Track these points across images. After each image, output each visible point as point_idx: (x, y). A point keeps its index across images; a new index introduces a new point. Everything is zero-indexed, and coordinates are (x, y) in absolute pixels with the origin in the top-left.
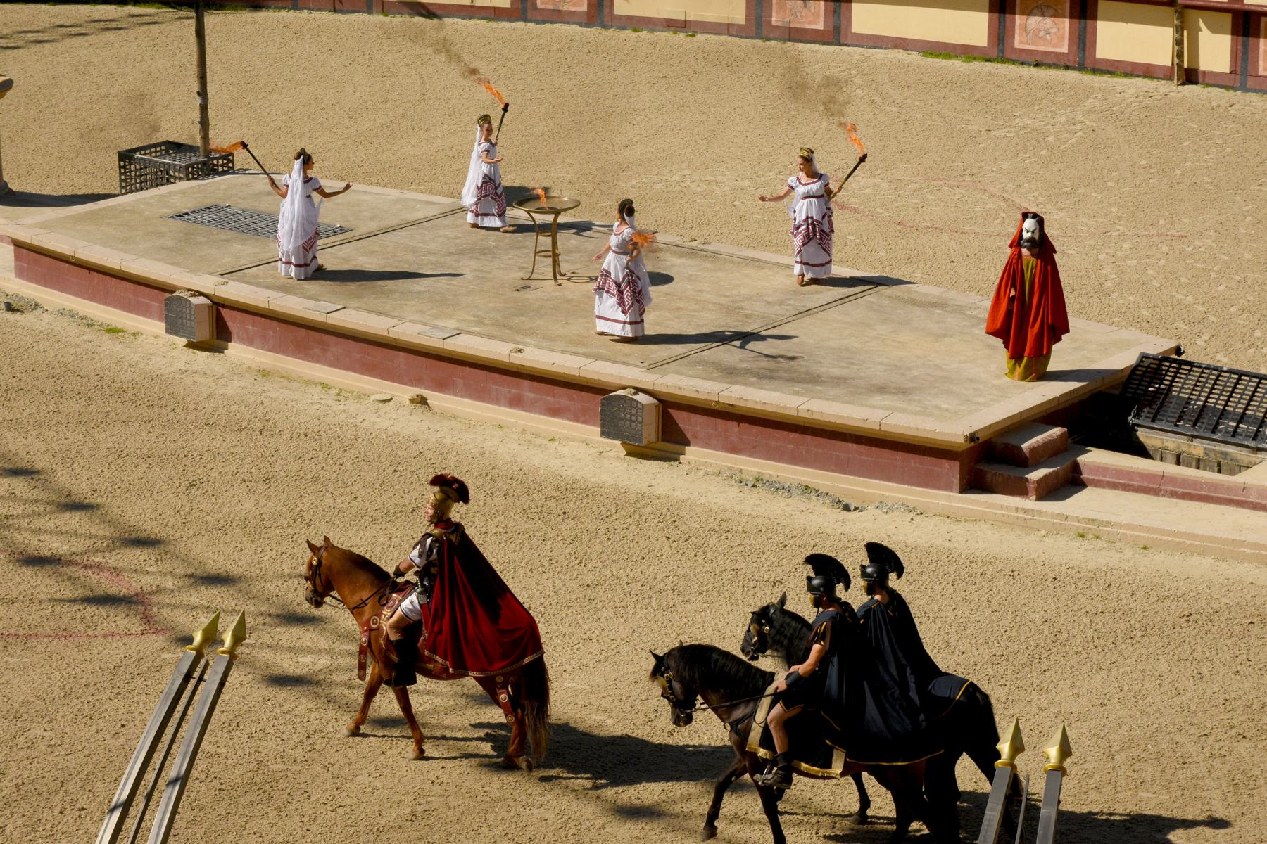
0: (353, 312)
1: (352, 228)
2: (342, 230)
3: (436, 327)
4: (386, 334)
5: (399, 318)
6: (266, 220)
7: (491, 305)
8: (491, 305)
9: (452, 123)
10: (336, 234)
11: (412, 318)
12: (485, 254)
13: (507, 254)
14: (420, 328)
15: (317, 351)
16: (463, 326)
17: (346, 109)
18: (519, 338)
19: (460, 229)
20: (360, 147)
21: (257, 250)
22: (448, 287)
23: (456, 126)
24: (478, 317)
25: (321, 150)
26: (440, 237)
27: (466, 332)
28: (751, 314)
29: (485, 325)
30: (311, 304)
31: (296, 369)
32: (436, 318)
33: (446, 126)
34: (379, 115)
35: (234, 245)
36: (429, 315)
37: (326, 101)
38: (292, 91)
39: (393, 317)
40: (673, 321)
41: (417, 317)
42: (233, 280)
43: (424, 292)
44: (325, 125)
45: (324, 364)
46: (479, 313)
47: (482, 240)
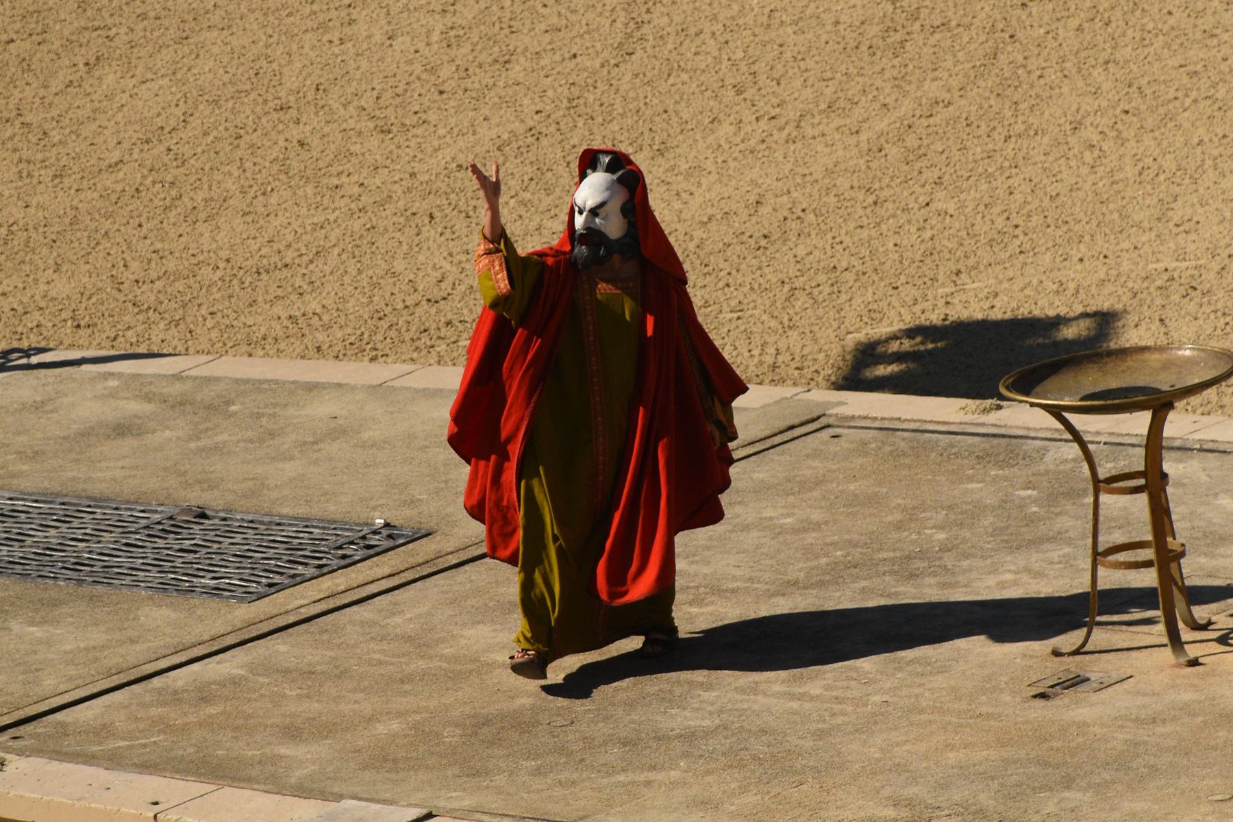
1: (426, 527)
6: (121, 524)
7: (952, 757)
8: (952, 757)
9: (748, 116)
10: (372, 552)
12: (913, 576)
13: (994, 571)
17: (367, 101)
19: (816, 494)
20: (429, 232)
21: (97, 636)
22: (795, 705)
23: (763, 124)
24: (910, 803)
25: (290, 256)
33: (726, 129)
34: (486, 111)
35: (15, 626)
37: (291, 82)
38: (167, 55)
42: (20, 753)
43: (708, 733)
44: (295, 165)
46: (912, 791)
47: (899, 526)
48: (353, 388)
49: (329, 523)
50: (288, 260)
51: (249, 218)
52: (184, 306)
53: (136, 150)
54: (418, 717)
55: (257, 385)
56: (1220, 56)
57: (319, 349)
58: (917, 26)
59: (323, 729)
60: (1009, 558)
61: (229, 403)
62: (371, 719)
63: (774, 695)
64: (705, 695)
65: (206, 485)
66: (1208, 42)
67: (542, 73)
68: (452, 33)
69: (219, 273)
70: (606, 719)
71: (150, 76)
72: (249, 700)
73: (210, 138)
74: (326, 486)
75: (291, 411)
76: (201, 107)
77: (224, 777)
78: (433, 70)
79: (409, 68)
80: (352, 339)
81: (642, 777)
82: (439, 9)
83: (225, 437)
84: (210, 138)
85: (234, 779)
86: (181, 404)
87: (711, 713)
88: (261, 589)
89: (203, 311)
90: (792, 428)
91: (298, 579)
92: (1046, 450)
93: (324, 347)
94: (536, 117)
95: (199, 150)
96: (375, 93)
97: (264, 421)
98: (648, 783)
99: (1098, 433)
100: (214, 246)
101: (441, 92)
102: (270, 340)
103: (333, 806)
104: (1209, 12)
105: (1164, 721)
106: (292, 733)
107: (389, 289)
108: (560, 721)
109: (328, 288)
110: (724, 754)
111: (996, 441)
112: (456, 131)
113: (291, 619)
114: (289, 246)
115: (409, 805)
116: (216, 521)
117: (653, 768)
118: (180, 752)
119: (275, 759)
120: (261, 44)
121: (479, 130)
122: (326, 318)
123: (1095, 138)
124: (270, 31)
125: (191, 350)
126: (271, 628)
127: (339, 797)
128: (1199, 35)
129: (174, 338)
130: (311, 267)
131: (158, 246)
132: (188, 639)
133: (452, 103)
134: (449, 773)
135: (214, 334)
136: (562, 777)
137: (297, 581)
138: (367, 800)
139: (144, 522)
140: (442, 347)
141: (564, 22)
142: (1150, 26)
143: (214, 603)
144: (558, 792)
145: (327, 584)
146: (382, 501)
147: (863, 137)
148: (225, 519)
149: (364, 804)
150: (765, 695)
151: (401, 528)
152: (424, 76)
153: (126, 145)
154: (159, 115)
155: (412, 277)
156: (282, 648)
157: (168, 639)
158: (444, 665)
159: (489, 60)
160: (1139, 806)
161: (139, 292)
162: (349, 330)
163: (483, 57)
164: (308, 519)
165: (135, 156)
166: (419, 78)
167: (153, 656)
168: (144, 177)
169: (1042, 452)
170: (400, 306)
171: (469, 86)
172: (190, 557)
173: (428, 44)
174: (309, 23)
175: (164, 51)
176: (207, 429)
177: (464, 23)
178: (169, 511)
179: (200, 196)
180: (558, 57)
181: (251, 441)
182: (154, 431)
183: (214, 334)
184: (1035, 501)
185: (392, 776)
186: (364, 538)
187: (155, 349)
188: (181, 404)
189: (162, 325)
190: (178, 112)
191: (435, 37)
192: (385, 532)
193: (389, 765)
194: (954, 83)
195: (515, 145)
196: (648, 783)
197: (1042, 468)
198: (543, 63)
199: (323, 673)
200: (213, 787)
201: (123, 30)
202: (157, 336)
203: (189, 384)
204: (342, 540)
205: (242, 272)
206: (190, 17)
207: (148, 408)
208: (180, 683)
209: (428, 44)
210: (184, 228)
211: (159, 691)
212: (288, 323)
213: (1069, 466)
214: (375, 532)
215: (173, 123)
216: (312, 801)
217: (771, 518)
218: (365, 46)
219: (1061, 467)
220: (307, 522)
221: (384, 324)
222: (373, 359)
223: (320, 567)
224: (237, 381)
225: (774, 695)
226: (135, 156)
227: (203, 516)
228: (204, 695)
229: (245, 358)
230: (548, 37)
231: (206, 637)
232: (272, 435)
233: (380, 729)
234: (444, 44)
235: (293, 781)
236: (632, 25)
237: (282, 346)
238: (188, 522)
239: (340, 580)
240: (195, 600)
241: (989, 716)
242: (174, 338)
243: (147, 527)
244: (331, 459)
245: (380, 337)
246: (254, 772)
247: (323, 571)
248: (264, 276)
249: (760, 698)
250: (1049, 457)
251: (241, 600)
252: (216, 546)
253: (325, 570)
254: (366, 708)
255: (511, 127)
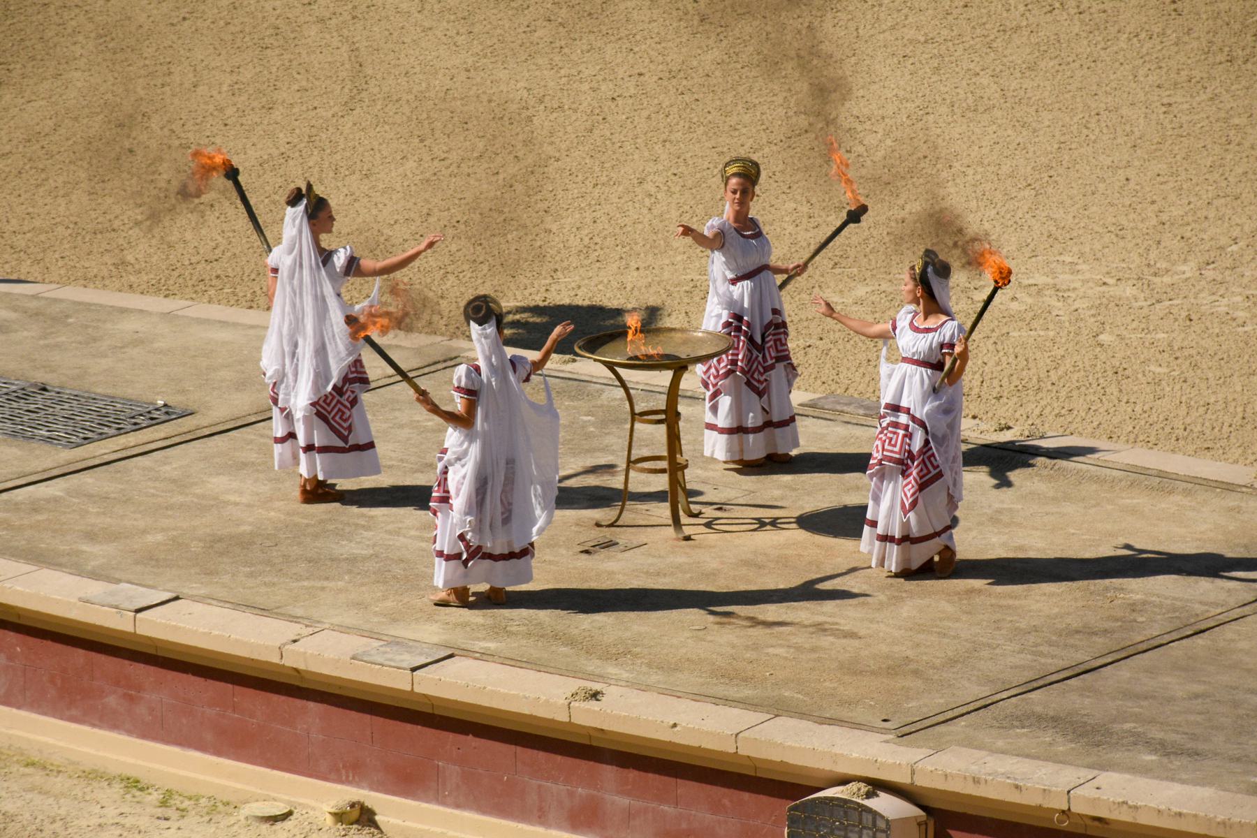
0: (198, 608)
1: (190, 409)
2: (170, 413)
3: (397, 642)
4: (275, 659)
5: (309, 621)
9: (427, 157)
10: (154, 422)
11: (336, 620)
14: (356, 643)
15: (112, 701)
16: (460, 639)
18: (592, 665)
23: (436, 162)
25: (116, 224)
26: (401, 426)
27: (467, 653)
28: (1144, 603)
29: (510, 634)
30: (95, 588)
31: (61, 744)
32: (395, 620)
33: (411, 164)
34: (254, 139)
36: (376, 614)
38: (47, 85)
39: (294, 619)
40: (958, 620)
41: (350, 618)
43: (365, 559)
45: (129, 732)
48: (150, 314)
49: (128, 401)
50: (115, 226)
51: (92, 197)
52: (44, 251)
53: (21, 146)
54: (175, 533)
55: (87, 306)
56: (740, 142)
57: (131, 286)
58: (542, 107)
59: (112, 536)
60: (572, 460)
61: (67, 317)
62: (145, 532)
63: (410, 537)
64: (366, 534)
65: (48, 369)
66: (732, 133)
67: (293, 118)
68: (236, 86)
69: (69, 231)
70: (299, 544)
71: (34, 98)
72: (65, 513)
73: (71, 142)
74: (127, 377)
75: (109, 326)
76: (66, 121)
77: (43, 562)
78: (221, 110)
79: (207, 107)
80: (153, 282)
81: (319, 584)
82: (228, 70)
83: (63, 339)
84: (71, 142)
85: (50, 563)
86: (37, 314)
87: (368, 546)
88: (79, 441)
89: (57, 256)
90: (435, 363)
91: (104, 436)
92: (603, 391)
93: (135, 286)
94: (287, 146)
95: (62, 149)
96: (182, 122)
97: (90, 330)
98: (323, 589)
99: (637, 383)
100: (68, 213)
101: (226, 125)
102: (99, 278)
103: (113, 587)
104: (735, 113)
105: (665, 575)
106: (91, 536)
107: (180, 251)
108: (268, 543)
109: (141, 247)
110: (374, 573)
111: (571, 382)
112: (233, 151)
113: (97, 462)
114: (116, 217)
115: (164, 590)
116: (53, 394)
117: (327, 579)
118: (16, 544)
119: (79, 553)
120: (109, 83)
121: (248, 152)
122: (137, 267)
123: (653, 190)
124: (116, 75)
125: (47, 280)
126: (84, 466)
127: (118, 581)
128: (726, 128)
129: (36, 272)
130: (131, 232)
131: (31, 210)
132: (28, 469)
133: (232, 132)
134: (193, 571)
135: (63, 272)
136: (266, 580)
137: (103, 437)
138: (137, 584)
139: (5, 390)
140: (212, 292)
141: (310, 85)
142: (695, 120)
143: (47, 447)
144: (263, 589)
145: (123, 441)
146: (164, 390)
147: (501, 177)
148: (58, 393)
149: (134, 587)
150: (405, 537)
151: (174, 408)
152: (216, 113)
153: (15, 142)
154: (38, 124)
155: (196, 244)
156: (90, 480)
157: (14, 469)
158: (195, 500)
159: (260, 106)
160: (643, 629)
161: (15, 239)
162: (152, 276)
163: (255, 104)
164: (113, 397)
165: (20, 150)
166: (212, 114)
167: (4, 479)
168: (25, 164)
169: (601, 392)
170: (187, 263)
171: (244, 122)
172: (33, 416)
173: (220, 93)
174: (142, 72)
175: (45, 82)
176: (52, 333)
177: (245, 80)
178: (22, 384)
179: (61, 180)
180: (304, 108)
181: (80, 343)
182: (16, 331)
183: (63, 272)
184: (593, 424)
185: (155, 570)
186: (149, 412)
187: (23, 278)
188: (37, 314)
189: (29, 262)
190: (50, 123)
191: (225, 88)
192: (164, 410)
193: (153, 563)
194: (563, 146)
195: (271, 163)
196: (323, 589)
197: (599, 402)
198: (294, 111)
199: (115, 499)
200: (34, 568)
201: (18, 66)
202: (24, 271)
203: (43, 302)
204: (134, 413)
205: (84, 232)
206: (63, 61)
207: (13, 315)
208: (20, 498)
209: (220, 93)
210: (49, 200)
211: (6, 502)
212: (112, 268)
213: (617, 403)
214: (157, 409)
215: (47, 130)
216: (100, 582)
217: (418, 421)
218: (178, 90)
219: (612, 403)
220: (113, 399)
221: (176, 274)
222: (166, 296)
223: (119, 429)
224: (75, 303)
225: (410, 537)
226: (20, 150)
227: (45, 389)
228: (35, 507)
229: (82, 289)
230: (299, 94)
231: (39, 469)
232: (95, 340)
233: (150, 538)
234: (230, 93)
235: (89, 568)
236: (355, 91)
237: (107, 282)
238: (34, 392)
239: (132, 439)
240: (34, 444)
241: (550, 562)
242: (36, 272)
243: (6, 394)
244: (132, 359)
245: (171, 282)
246: (64, 560)
247: (120, 432)
248: (99, 236)
249: (402, 539)
250: (604, 396)
251: (65, 446)
252: (51, 410)
253: (122, 431)
254: (141, 524)
255: (270, 151)
